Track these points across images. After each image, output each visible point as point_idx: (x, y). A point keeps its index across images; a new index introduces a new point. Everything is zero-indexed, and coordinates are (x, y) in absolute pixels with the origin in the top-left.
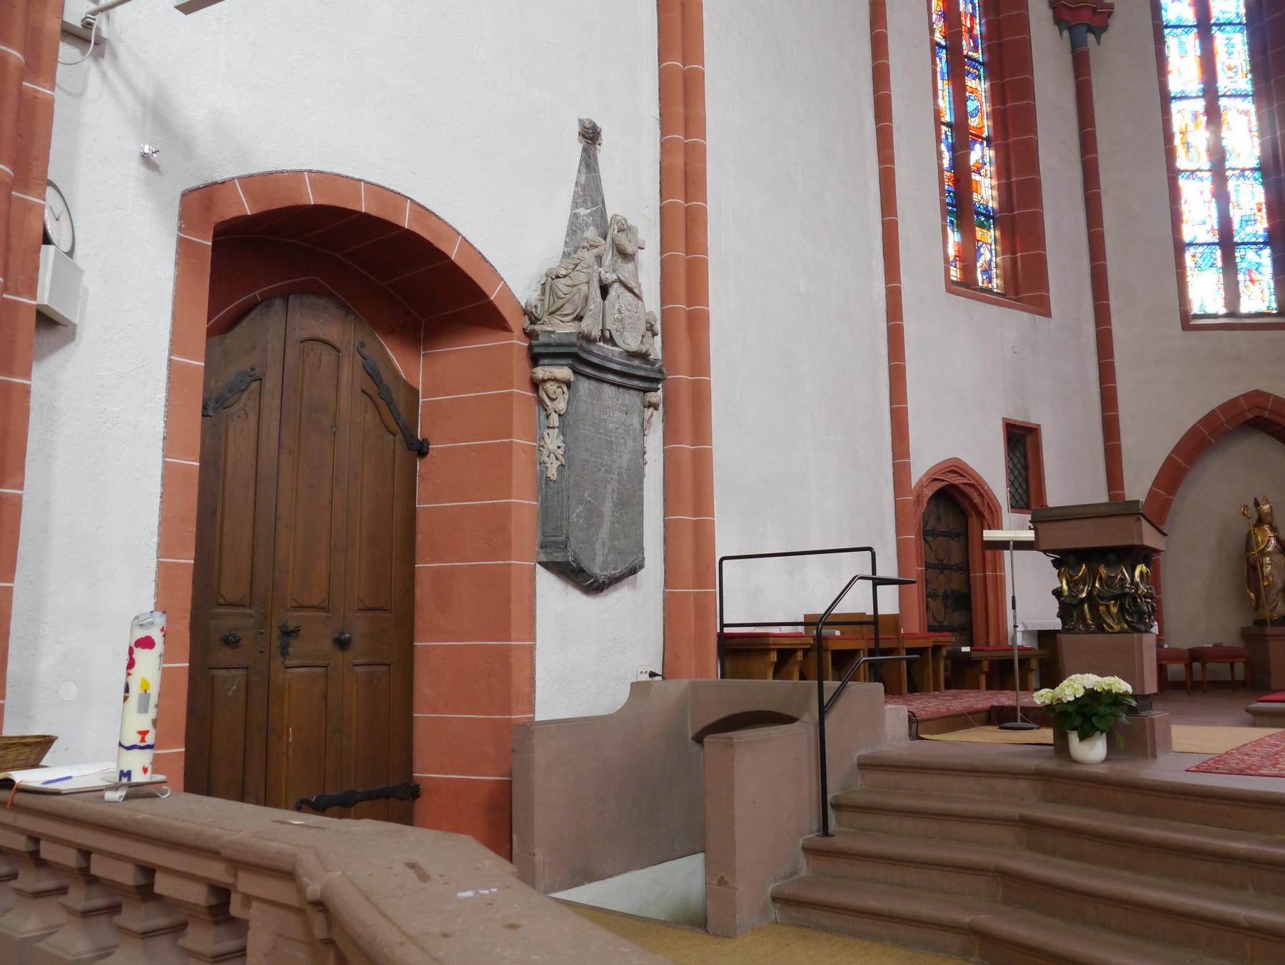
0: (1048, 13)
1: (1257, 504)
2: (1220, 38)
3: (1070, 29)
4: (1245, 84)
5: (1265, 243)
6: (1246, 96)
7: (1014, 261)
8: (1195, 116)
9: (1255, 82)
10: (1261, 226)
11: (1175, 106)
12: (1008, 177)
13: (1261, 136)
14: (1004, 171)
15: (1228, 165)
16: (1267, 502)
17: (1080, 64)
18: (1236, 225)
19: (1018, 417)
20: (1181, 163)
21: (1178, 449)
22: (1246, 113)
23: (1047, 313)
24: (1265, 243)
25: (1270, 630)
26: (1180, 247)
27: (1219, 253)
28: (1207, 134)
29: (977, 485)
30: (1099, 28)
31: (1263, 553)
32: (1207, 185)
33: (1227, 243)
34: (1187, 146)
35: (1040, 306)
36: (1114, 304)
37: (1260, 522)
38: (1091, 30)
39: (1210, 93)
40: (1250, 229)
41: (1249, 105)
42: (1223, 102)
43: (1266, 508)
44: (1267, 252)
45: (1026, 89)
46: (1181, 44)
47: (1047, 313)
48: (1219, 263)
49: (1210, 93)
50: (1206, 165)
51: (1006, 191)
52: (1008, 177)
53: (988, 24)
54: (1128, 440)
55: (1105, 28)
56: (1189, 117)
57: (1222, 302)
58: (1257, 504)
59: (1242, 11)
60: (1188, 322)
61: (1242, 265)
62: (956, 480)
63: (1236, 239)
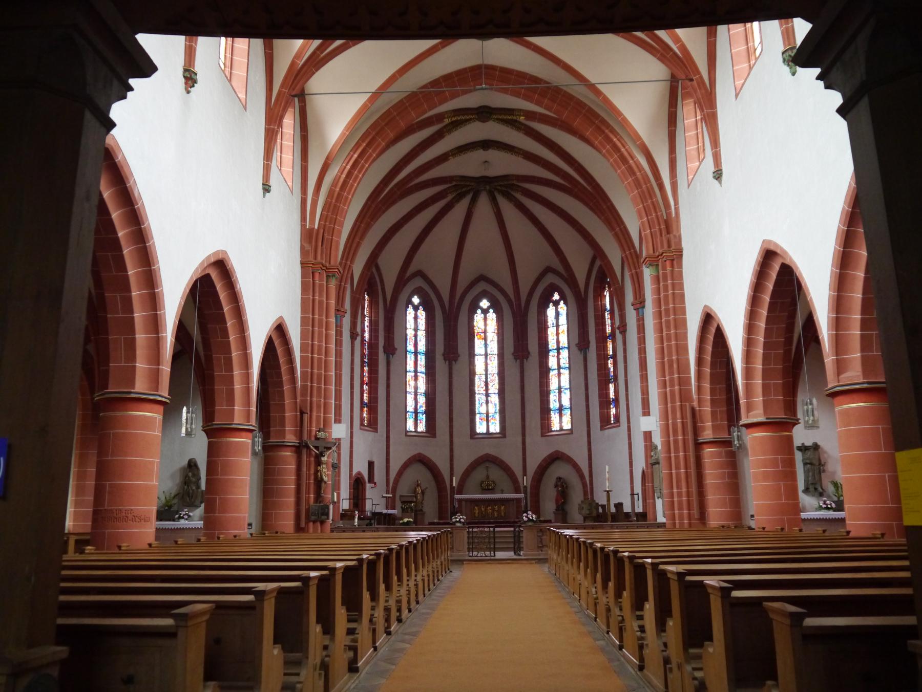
0: (383, 350)
1: (417, 481)
2: (419, 356)
3: (387, 354)
4: (423, 370)
5: (424, 413)
6: (423, 373)
7: (370, 417)
8: (412, 376)
9: (426, 369)
10: (424, 409)
11: (408, 374)
12: (371, 395)
13: (426, 385)
14: (370, 393)
15: (418, 391)
16: (420, 480)
17: (388, 364)
18: (418, 408)
19: (370, 460)
20: (408, 390)
21: (402, 467)
22: (423, 378)
23: (377, 432)
24: (424, 413)
25: (418, 512)
26: (406, 412)
27: (414, 415)
28: (414, 382)
29: (363, 477)
30: (393, 354)
31: (418, 493)
32: (413, 396)
33: (416, 412)
34: (409, 385)
35: (376, 430)
36: (391, 428)
37: (418, 485)
38: (391, 354)
39: (416, 371)
40: (421, 409)
41: (424, 376)
42: (418, 374)
43: (419, 482)
44: (425, 415)
45: (377, 372)
46: (410, 357)
47: (377, 432)
48: (414, 417)
49: (416, 371)
50: (413, 391)
51: (370, 398)
52: (371, 395)
53: (369, 352)
54: (391, 464)
55: (395, 354)
56: (410, 377)
57: (413, 427)
58: (417, 481)
59: (425, 350)
60: (407, 432)
61: (419, 418)
62: (359, 476)
63: (418, 411)
